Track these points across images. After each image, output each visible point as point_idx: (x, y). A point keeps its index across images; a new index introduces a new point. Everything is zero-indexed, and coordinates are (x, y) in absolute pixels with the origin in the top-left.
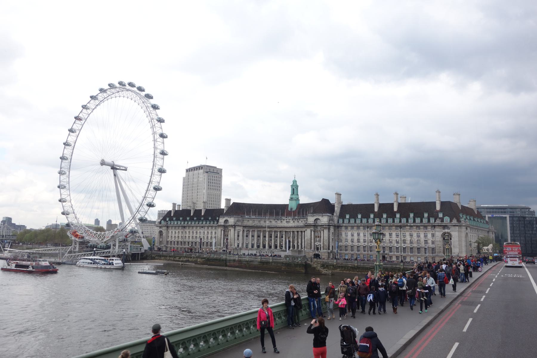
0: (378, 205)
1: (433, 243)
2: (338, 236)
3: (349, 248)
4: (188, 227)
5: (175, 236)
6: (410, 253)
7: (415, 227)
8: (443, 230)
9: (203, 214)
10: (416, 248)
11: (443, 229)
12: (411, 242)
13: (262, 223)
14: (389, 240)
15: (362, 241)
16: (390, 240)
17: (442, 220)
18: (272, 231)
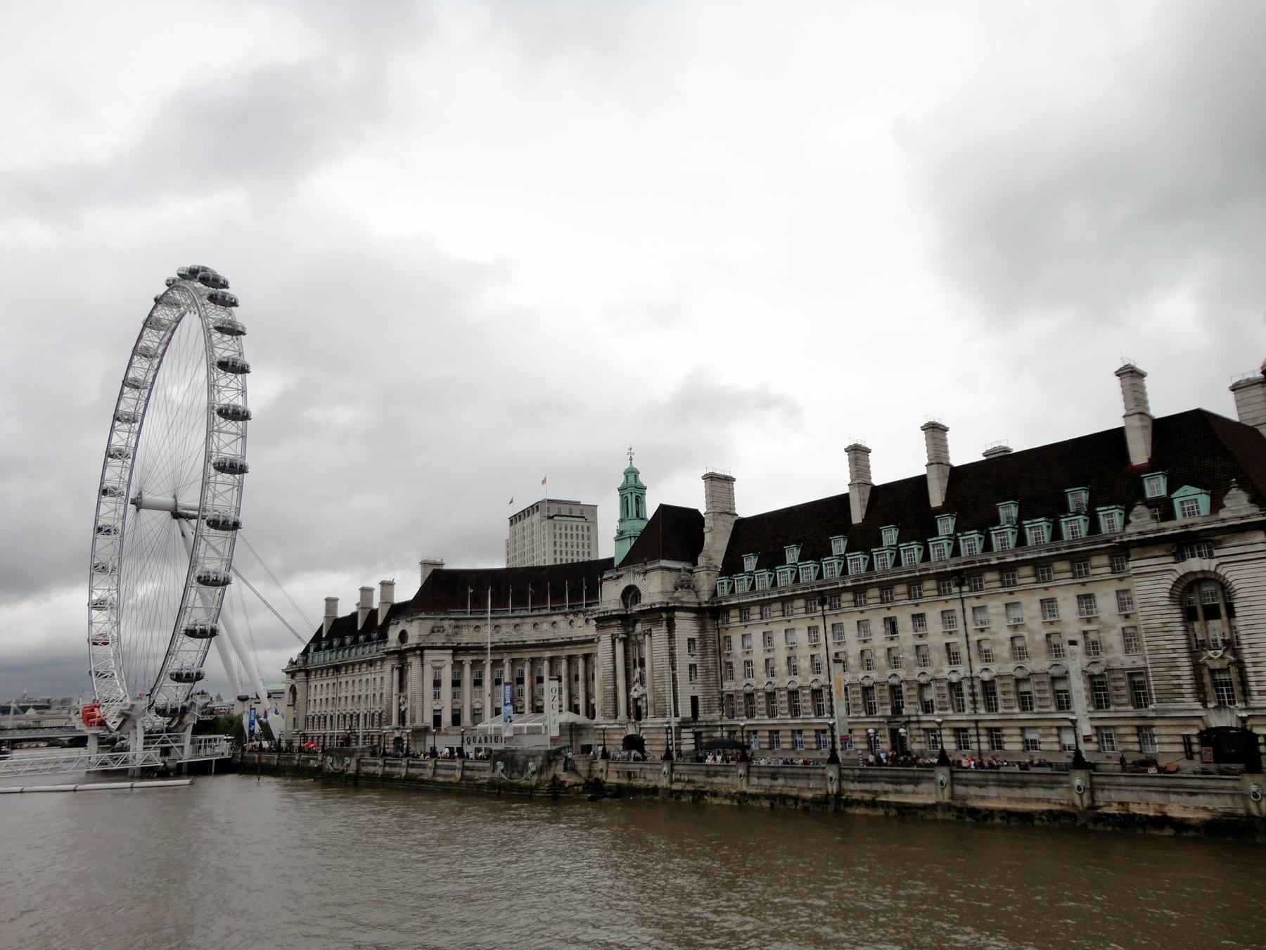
0: (867, 495)
1: (1130, 640)
2: (718, 653)
3: (760, 703)
4: (344, 668)
5: (321, 700)
6: (1017, 710)
7: (1027, 571)
8: (1175, 566)
9: (380, 623)
10: (1046, 679)
11: (1171, 559)
12: (1019, 652)
13: (528, 633)
14: (914, 650)
15: (804, 664)
16: (917, 647)
17: (1164, 509)
18: (559, 658)
